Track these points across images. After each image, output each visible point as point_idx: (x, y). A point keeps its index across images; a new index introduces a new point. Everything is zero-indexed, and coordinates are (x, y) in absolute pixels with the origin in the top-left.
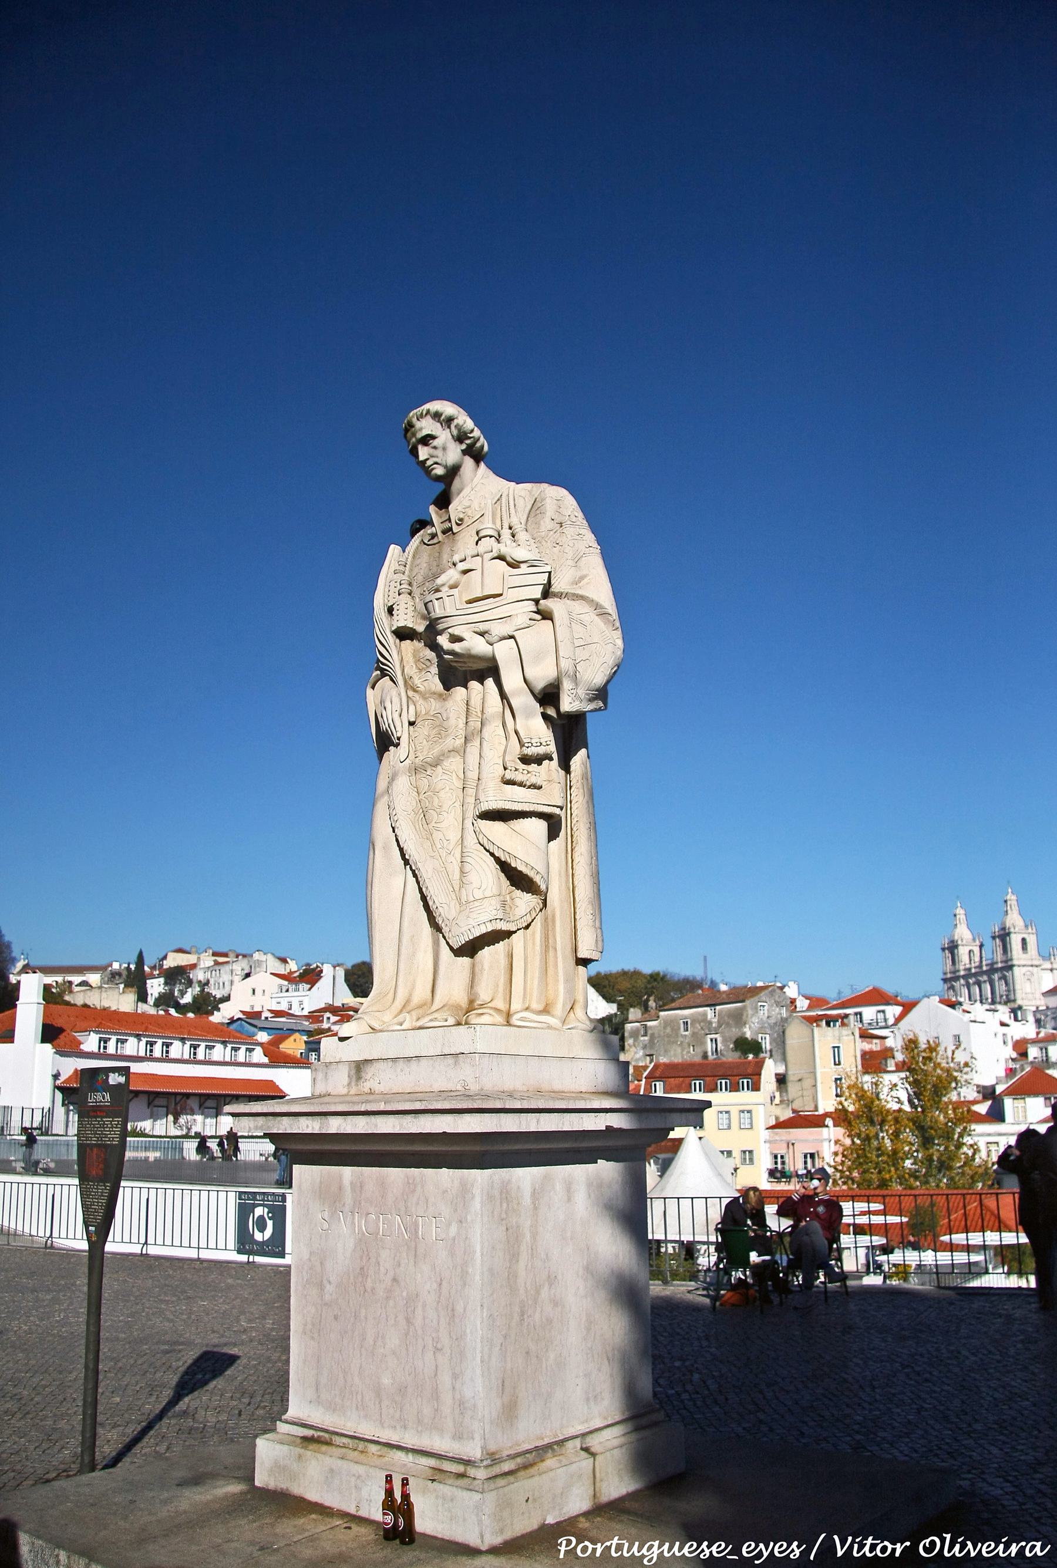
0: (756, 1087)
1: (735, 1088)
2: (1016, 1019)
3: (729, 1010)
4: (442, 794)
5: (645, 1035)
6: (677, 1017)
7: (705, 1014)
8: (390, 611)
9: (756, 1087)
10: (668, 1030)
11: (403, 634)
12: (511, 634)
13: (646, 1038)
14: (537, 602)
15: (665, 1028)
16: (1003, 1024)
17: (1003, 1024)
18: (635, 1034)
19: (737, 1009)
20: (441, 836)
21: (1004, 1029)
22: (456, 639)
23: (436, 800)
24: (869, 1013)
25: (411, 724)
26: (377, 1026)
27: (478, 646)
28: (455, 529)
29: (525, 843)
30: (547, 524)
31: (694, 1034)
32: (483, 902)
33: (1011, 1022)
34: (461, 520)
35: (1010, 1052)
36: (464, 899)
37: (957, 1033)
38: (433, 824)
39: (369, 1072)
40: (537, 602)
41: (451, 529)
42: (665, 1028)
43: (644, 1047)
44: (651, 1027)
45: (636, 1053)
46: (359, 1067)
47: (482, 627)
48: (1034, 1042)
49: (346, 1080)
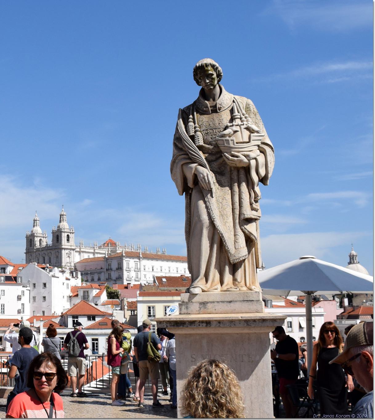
2: (73, 277)
4: (227, 210)
8: (193, 138)
11: (200, 148)
12: (255, 157)
14: (258, 146)
16: (67, 279)
17: (67, 279)
20: (228, 225)
21: (68, 281)
22: (233, 156)
23: (225, 212)
25: (214, 183)
26: (206, 289)
27: (245, 160)
28: (218, 111)
30: (252, 115)
33: (70, 277)
34: (221, 107)
35: (69, 293)
36: (236, 248)
37: (44, 282)
38: (225, 221)
39: (209, 306)
40: (258, 146)
41: (216, 110)
46: (204, 304)
47: (246, 153)
48: (82, 288)
49: (198, 309)
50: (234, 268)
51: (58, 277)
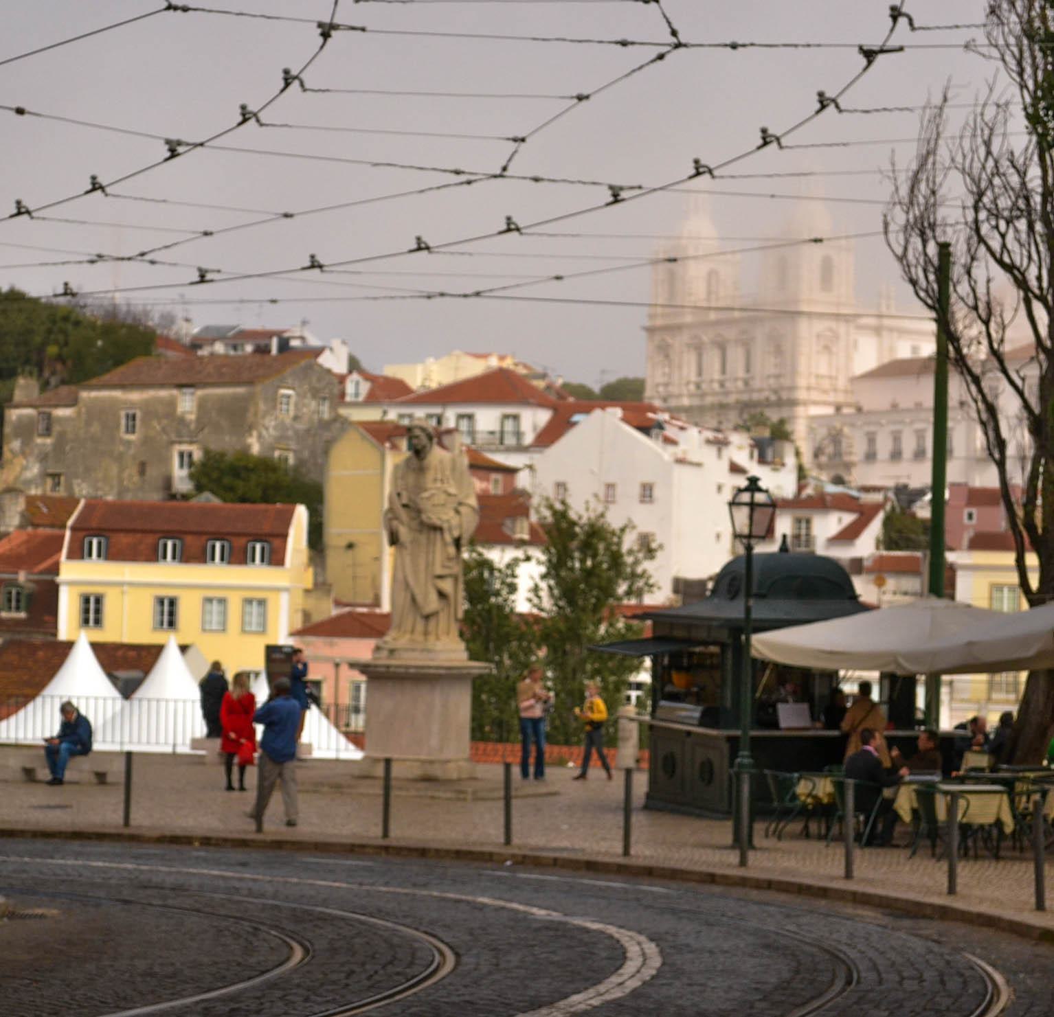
0: (275, 558)
1: (238, 557)
3: (221, 399)
5: (48, 432)
6: (114, 403)
7: (172, 404)
9: (275, 558)
10: (95, 428)
13: (49, 441)
15: (88, 423)
18: (26, 431)
19: (235, 398)
24: (487, 418)
29: (447, 586)
31: (146, 441)
32: (433, 603)
42: (88, 423)
43: (43, 458)
44: (61, 420)
45: (25, 468)
48: (786, 504)
50: (427, 617)
51: (699, 465)
